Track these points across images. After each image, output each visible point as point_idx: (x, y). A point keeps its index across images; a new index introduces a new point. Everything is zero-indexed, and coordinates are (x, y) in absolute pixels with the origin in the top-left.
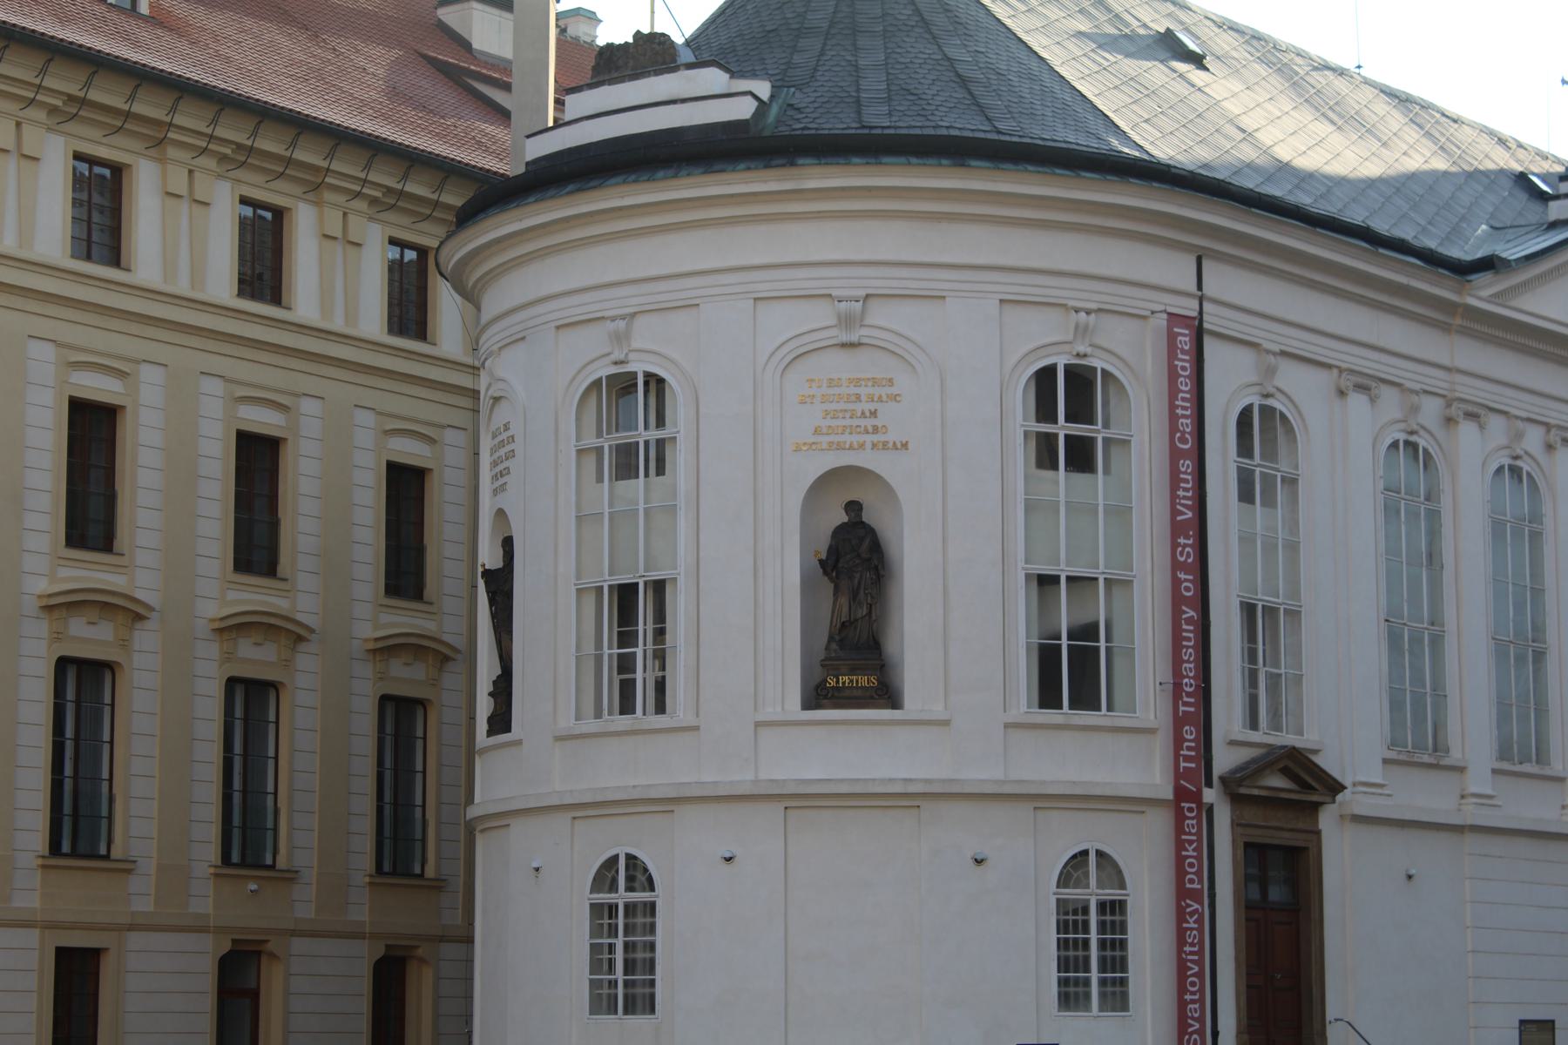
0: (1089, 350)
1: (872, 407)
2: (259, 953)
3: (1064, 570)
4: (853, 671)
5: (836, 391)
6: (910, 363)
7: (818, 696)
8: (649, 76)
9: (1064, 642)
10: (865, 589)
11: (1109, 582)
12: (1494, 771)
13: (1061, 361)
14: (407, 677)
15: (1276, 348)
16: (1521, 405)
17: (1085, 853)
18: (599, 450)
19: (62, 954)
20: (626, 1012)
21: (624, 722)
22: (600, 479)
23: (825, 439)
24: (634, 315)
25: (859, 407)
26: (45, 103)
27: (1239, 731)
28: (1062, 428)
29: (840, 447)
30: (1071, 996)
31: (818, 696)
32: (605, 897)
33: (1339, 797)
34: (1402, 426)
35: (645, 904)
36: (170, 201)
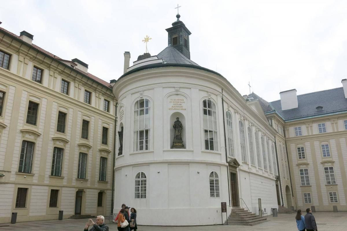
0: (210, 98)
1: (181, 103)
3: (209, 129)
4: (178, 143)
5: (175, 101)
7: (173, 147)
9: (209, 140)
13: (207, 99)
17: (213, 172)
18: (138, 111)
19: (52, 191)
20: (141, 198)
21: (141, 151)
23: (173, 108)
24: (144, 91)
25: (179, 104)
27: (229, 156)
28: (207, 109)
29: (176, 109)
30: (212, 195)
31: (173, 147)
32: (138, 179)
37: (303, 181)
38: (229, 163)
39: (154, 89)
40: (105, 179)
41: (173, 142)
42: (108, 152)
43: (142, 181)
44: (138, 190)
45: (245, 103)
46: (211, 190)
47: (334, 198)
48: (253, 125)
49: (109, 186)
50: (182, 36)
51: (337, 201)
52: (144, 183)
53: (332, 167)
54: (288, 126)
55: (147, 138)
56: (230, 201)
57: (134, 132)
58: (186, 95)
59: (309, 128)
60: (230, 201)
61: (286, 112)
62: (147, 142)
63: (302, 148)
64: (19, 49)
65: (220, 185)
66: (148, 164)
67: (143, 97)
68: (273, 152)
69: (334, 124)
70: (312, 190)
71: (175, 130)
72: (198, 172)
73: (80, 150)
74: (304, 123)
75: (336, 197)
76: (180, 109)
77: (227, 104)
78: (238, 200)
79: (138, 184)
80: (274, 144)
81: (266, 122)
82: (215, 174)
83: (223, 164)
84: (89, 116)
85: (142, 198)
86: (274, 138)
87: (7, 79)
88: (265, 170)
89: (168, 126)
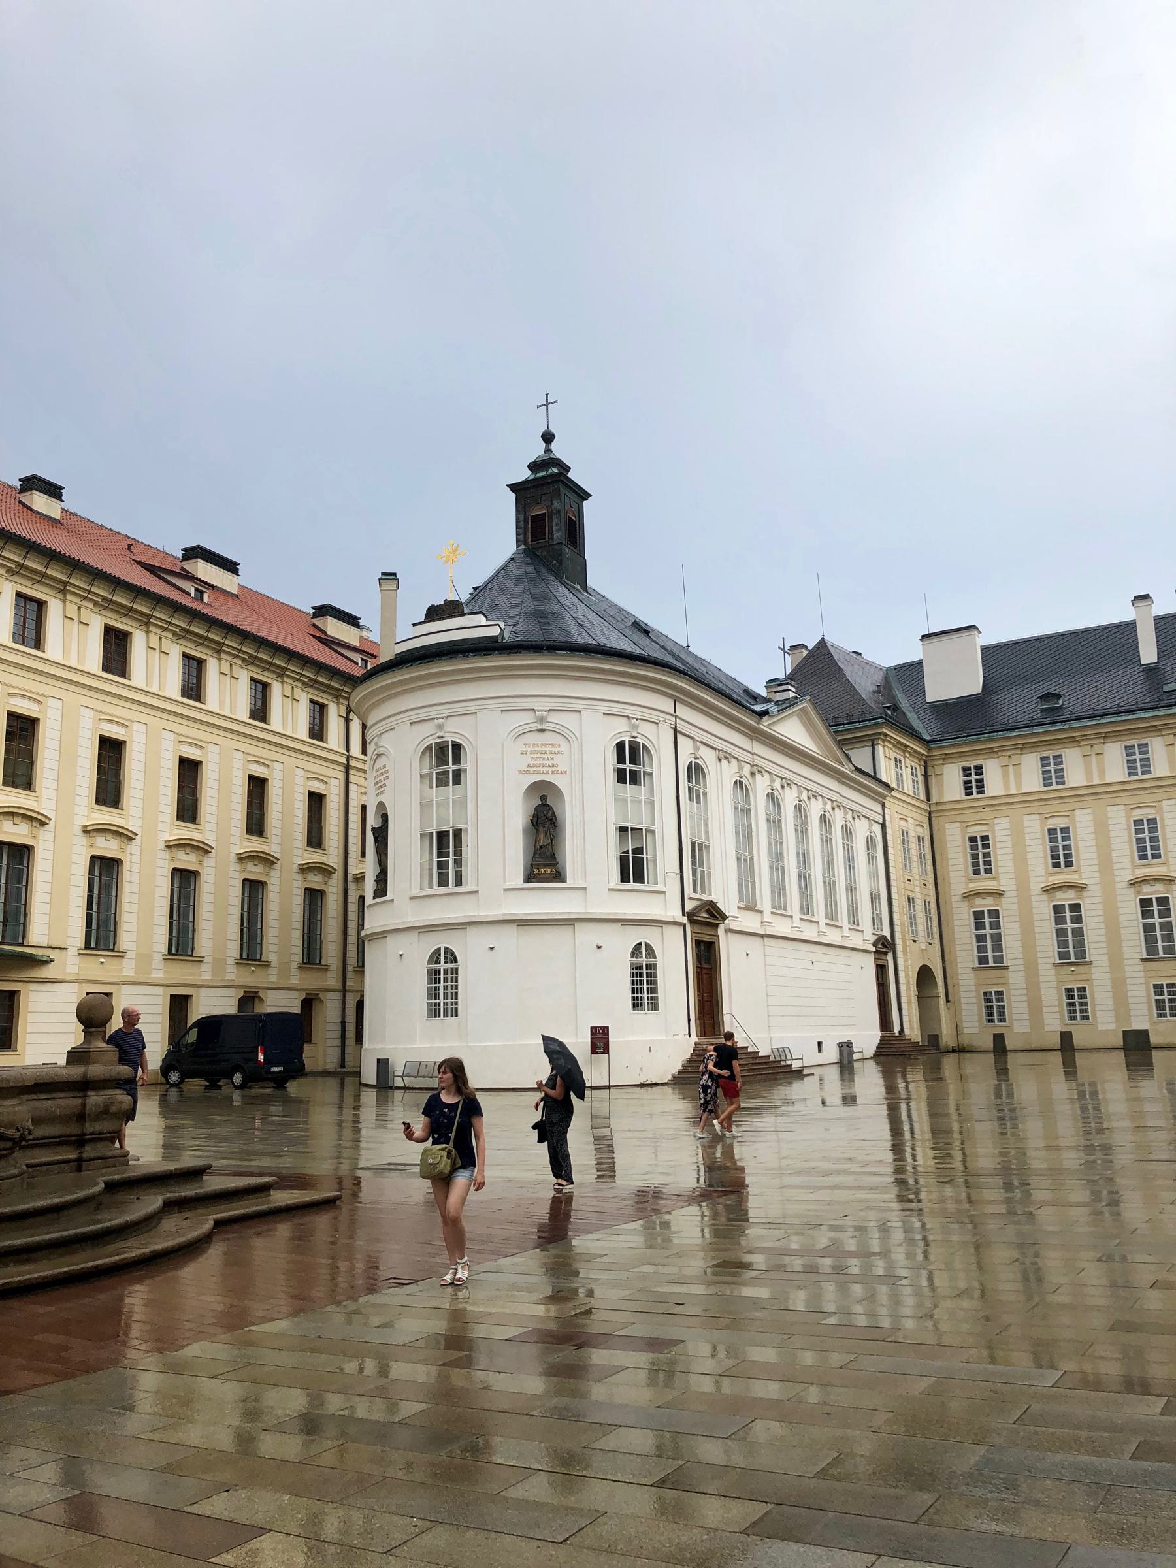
1: (552, 756)
2: (254, 997)
3: (630, 825)
4: (546, 866)
5: (537, 749)
7: (530, 877)
9: (631, 855)
12: (772, 913)
13: (627, 739)
15: (699, 740)
16: (775, 770)
17: (640, 944)
18: (430, 775)
19: (173, 998)
21: (443, 890)
22: (431, 787)
23: (532, 769)
25: (546, 756)
26: (172, 630)
28: (628, 767)
29: (538, 772)
30: (637, 1005)
33: (726, 922)
34: (738, 774)
35: (452, 969)
36: (222, 676)
37: (981, 949)
38: (690, 916)
41: (531, 865)
42: (325, 871)
44: (437, 997)
45: (756, 725)
47: (1077, 1008)
48: (787, 783)
49: (332, 979)
50: (559, 511)
51: (1087, 1018)
52: (452, 978)
53: (1079, 905)
54: (941, 762)
55: (458, 853)
56: (689, 1020)
58: (567, 731)
59: (1011, 769)
60: (689, 1020)
61: (945, 709)
62: (458, 863)
63: (985, 838)
64: (66, 583)
65: (660, 979)
66: (463, 926)
67: (447, 734)
68: (871, 859)
69: (1094, 758)
70: (1011, 981)
72: (600, 945)
73: (243, 871)
75: (1086, 1004)
77: (690, 742)
78: (720, 1017)
79: (435, 979)
80: (877, 829)
82: (646, 951)
83: (672, 920)
86: (878, 808)
87: (39, 678)
88: (828, 921)
89: (517, 817)
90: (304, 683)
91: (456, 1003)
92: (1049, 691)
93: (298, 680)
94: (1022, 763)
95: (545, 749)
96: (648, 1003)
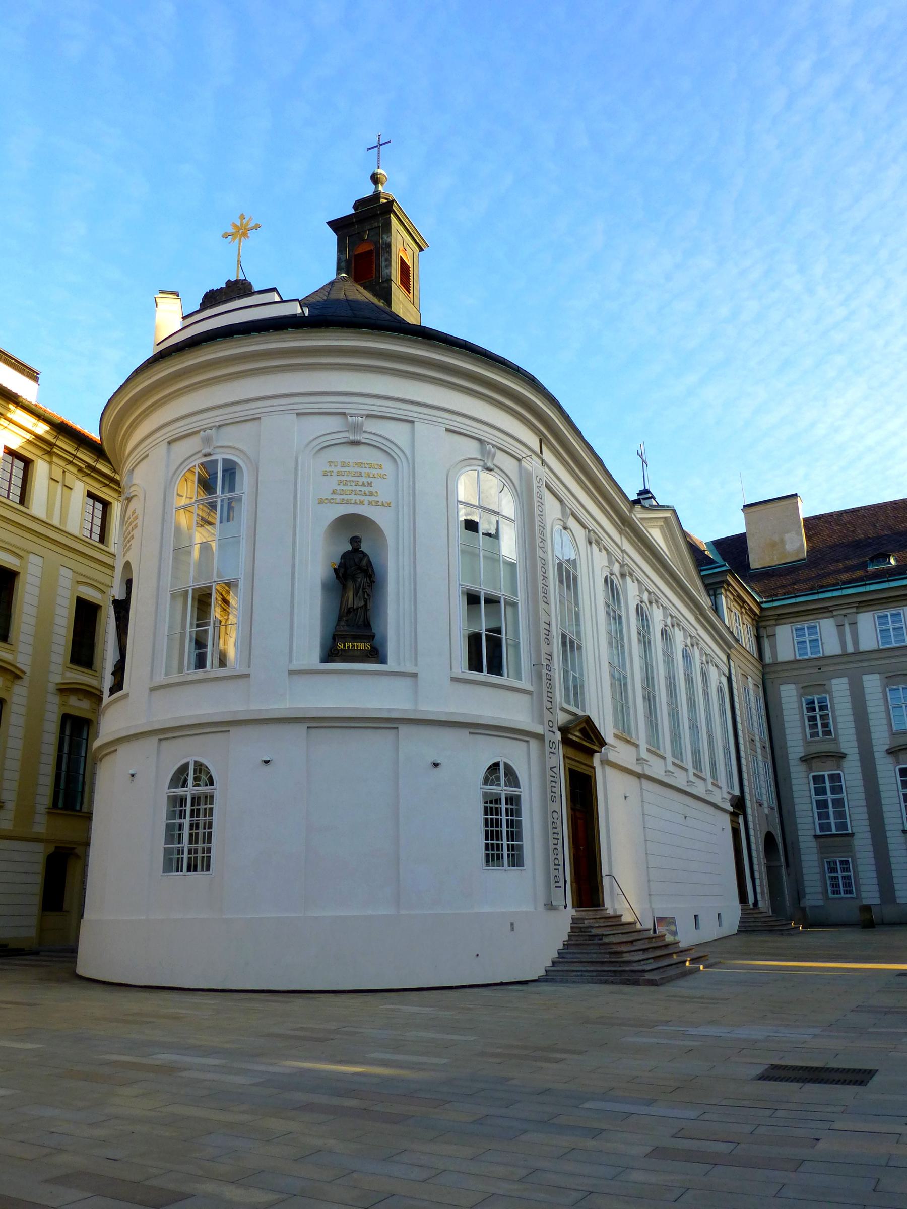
0: (492, 467)
1: (369, 480)
3: (484, 589)
4: (355, 638)
6: (393, 457)
7: (331, 654)
8: (235, 300)
10: (363, 589)
11: (506, 603)
14: (79, 706)
20: (189, 870)
21: (200, 674)
23: (338, 497)
25: (361, 480)
29: (348, 502)
30: (493, 857)
31: (331, 654)
32: (179, 791)
37: (823, 815)
39: (259, 418)
40: (82, 804)
43: (196, 800)
46: (487, 839)
54: (773, 622)
57: (173, 597)
59: (847, 628)
71: (344, 587)
74: (825, 610)
76: (366, 502)
81: (701, 596)
84: (21, 553)
85: (195, 870)
86: (724, 659)
88: (696, 772)
90: (80, 470)
91: (209, 850)
92: (881, 551)
93: (70, 463)
94: (858, 622)
95: (359, 470)
96: (508, 855)
